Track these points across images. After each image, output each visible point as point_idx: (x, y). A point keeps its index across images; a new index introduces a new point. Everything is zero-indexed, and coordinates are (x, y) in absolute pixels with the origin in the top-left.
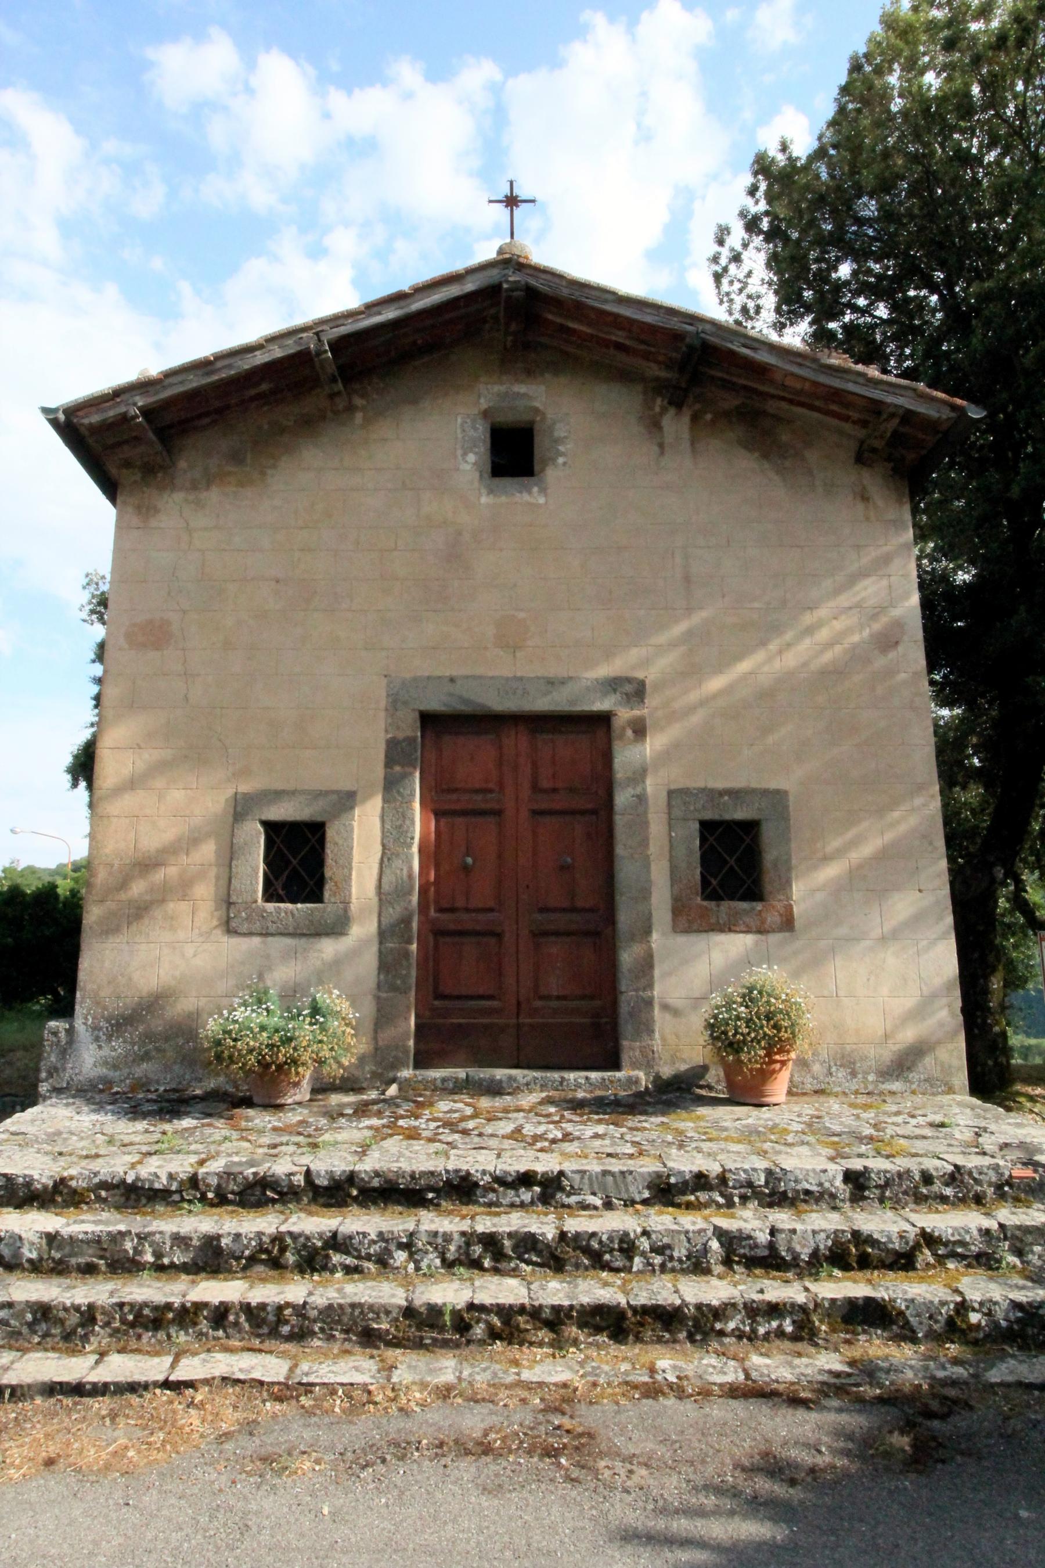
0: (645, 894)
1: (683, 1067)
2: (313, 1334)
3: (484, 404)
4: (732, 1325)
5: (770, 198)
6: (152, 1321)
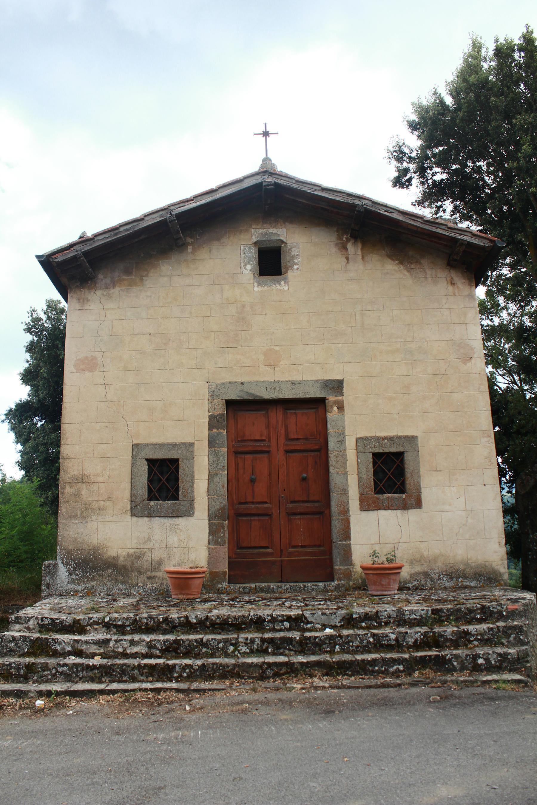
0: (345, 492)
3: (254, 239)
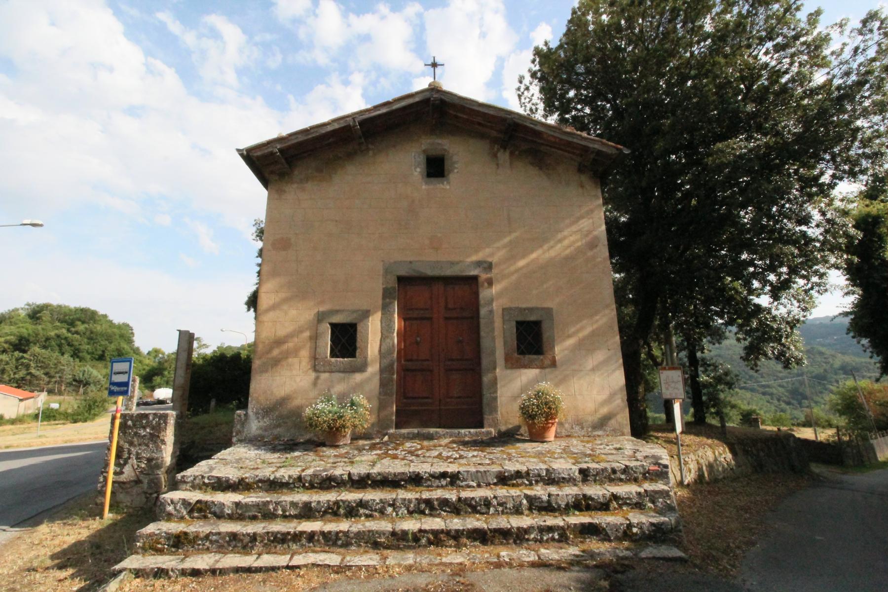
0: (493, 353)
1: (510, 426)
2: (351, 544)
3: (423, 147)
4: (532, 536)
5: (541, 64)
6: (281, 540)
